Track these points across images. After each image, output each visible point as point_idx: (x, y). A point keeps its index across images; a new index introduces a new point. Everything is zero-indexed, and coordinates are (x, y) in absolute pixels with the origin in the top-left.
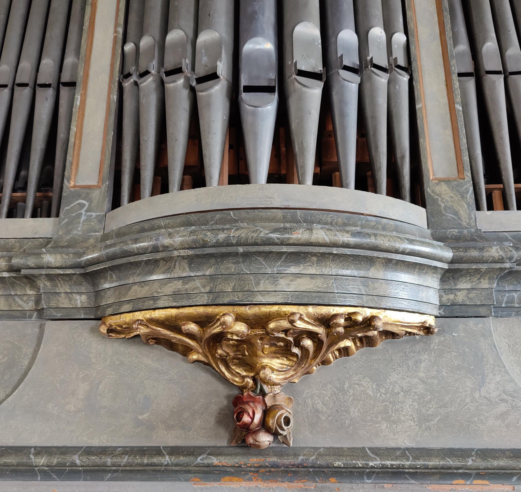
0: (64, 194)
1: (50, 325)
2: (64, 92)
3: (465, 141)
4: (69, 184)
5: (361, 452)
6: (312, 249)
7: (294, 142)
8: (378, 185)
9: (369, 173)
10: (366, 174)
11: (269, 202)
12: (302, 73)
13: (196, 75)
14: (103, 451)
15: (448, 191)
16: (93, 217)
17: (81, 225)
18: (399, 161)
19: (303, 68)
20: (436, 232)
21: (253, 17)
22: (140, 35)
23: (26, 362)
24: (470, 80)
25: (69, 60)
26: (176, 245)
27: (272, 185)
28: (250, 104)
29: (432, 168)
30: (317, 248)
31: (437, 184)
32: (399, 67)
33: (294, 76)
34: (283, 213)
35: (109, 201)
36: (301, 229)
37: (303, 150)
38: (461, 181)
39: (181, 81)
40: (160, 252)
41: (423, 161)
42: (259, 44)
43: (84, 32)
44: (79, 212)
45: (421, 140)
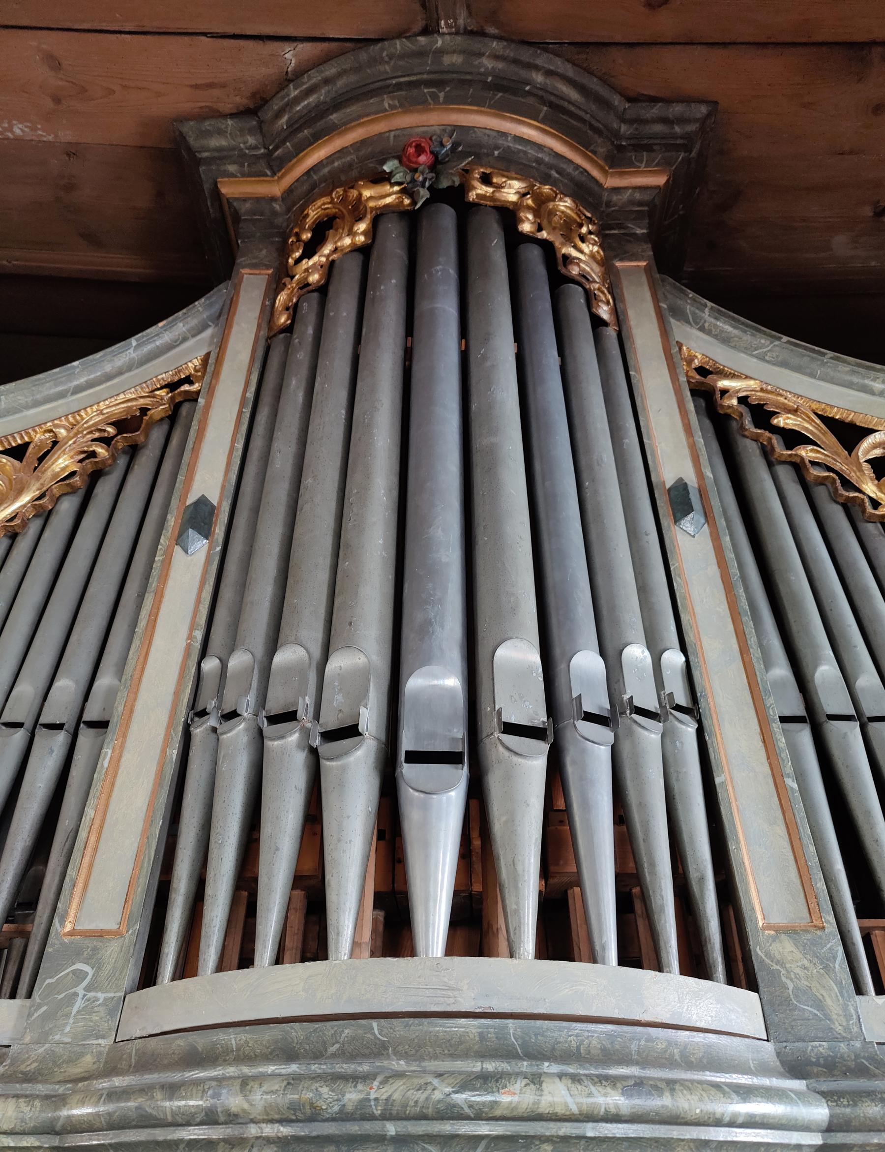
0: (49, 950)
2: (86, 737)
3: (812, 849)
4: (64, 927)
6: (542, 1127)
7: (499, 859)
8: (662, 944)
9: (636, 890)
10: (631, 890)
11: (452, 1000)
12: (510, 729)
13: (321, 726)
15: (798, 955)
16: (98, 1003)
17: (71, 1021)
18: (695, 888)
19: (513, 720)
20: (785, 1047)
21: (426, 628)
22: (232, 649)
24: (801, 731)
25: (104, 681)
26: (255, 1113)
27: (457, 960)
28: (415, 787)
29: (760, 903)
30: (552, 1125)
31: (774, 939)
32: (678, 708)
33: (497, 734)
34: (479, 1028)
35: (136, 964)
36: (519, 1082)
37: (516, 877)
38: (819, 933)
39: (294, 738)
40: (219, 1124)
41: (740, 890)
42: (437, 677)
43: (135, 636)
44: (73, 990)
45: (732, 846)
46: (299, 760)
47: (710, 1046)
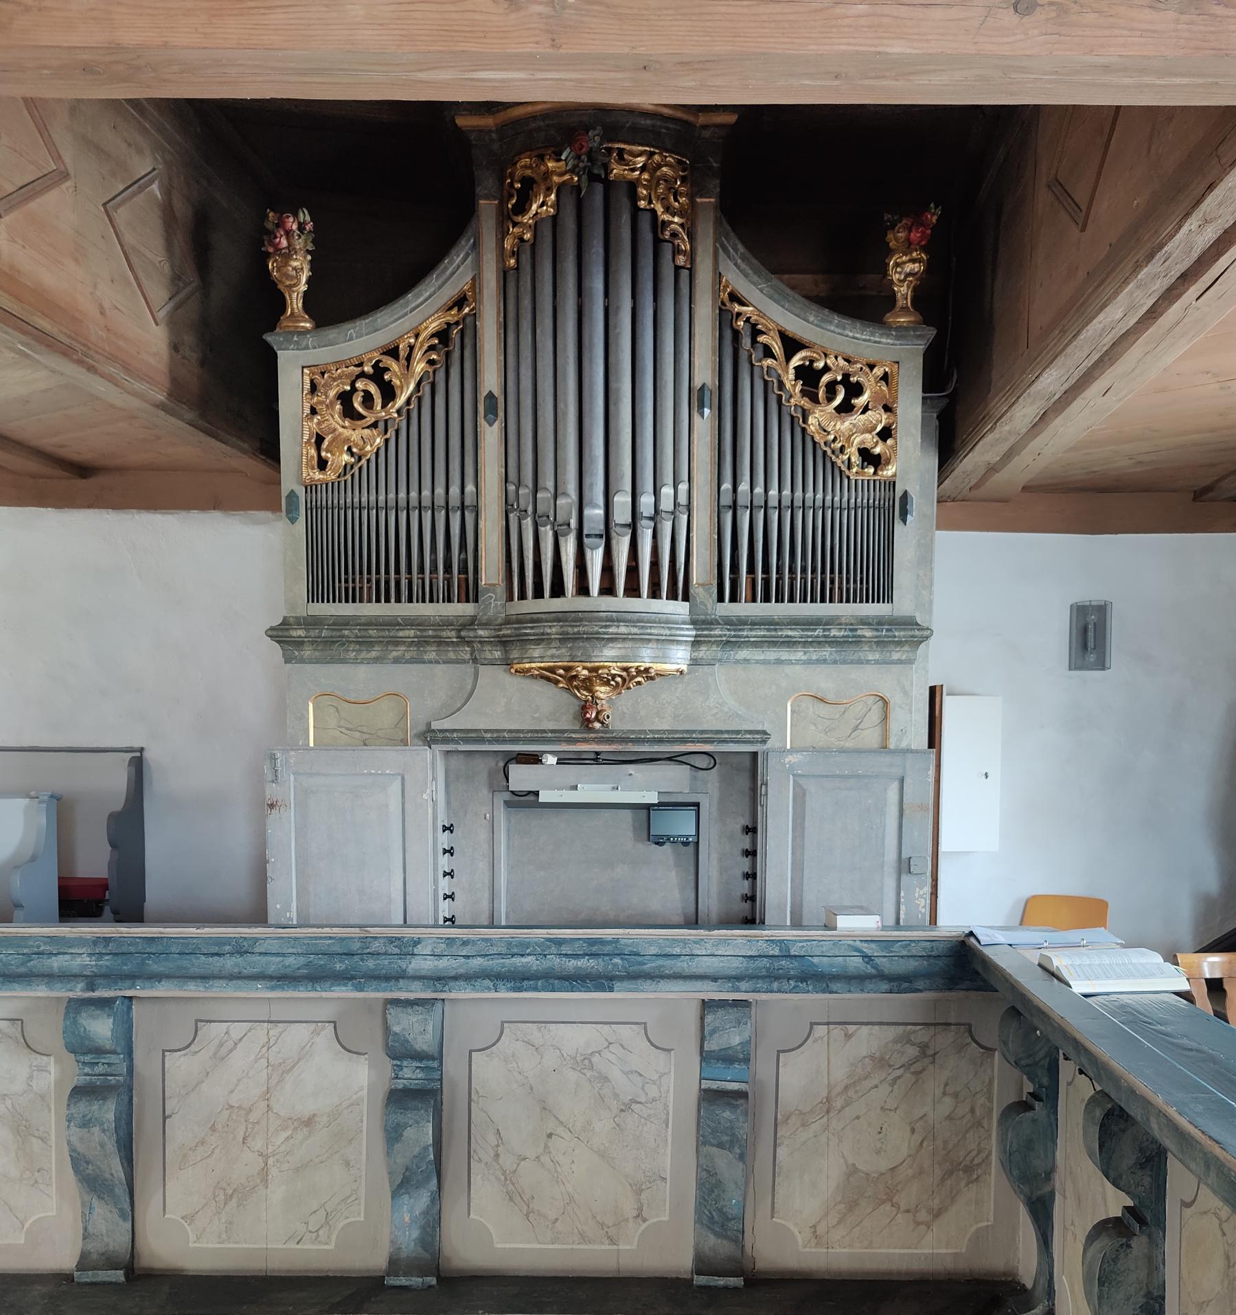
1: (481, 668)
5: (644, 732)
14: (518, 731)
23: (470, 687)
46: (550, 533)
47: (667, 618)
